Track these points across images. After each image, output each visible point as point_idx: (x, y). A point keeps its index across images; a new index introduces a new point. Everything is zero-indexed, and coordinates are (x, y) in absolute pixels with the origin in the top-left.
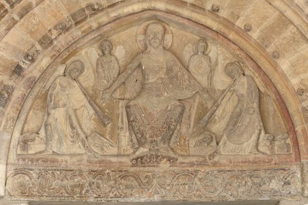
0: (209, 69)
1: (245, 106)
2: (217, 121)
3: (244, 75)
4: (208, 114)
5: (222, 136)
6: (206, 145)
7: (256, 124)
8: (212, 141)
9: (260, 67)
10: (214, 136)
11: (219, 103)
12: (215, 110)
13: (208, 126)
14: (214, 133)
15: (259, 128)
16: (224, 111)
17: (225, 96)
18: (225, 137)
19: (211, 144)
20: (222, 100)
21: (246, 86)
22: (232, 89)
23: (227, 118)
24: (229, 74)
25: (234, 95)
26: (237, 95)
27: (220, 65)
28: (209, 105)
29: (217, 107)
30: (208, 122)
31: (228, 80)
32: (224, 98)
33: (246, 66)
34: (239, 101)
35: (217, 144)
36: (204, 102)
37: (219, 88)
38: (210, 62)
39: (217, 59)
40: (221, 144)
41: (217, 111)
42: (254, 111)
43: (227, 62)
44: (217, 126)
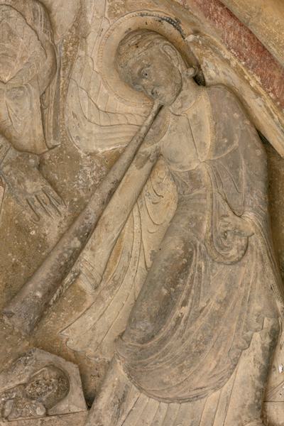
0: (48, 63)
1: (205, 227)
2: (90, 299)
3: (199, 81)
4: (44, 274)
5: (109, 366)
6: (40, 412)
7: (257, 306)
8: (64, 391)
9: (262, 50)
10: (72, 370)
11: (92, 218)
12: (76, 254)
13: (48, 323)
14: (75, 358)
15: (268, 323)
16: (116, 247)
17: (118, 183)
18: (119, 373)
19: (63, 407)
20: (105, 203)
21: (208, 137)
22: (148, 148)
23: (131, 283)
24: (134, 81)
25: (161, 174)
26: (172, 175)
27: (92, 38)
28: (52, 226)
29: (86, 235)
30: (44, 309)
31: (132, 110)
32: (111, 194)
33: (208, 44)
34: (181, 202)
35: (90, 401)
36: (28, 216)
37: (93, 148)
38: (51, 26)
39: (81, 13)
40: (103, 402)
41: (86, 255)
42: (246, 249)
43: (128, 22)
44: (90, 319)
